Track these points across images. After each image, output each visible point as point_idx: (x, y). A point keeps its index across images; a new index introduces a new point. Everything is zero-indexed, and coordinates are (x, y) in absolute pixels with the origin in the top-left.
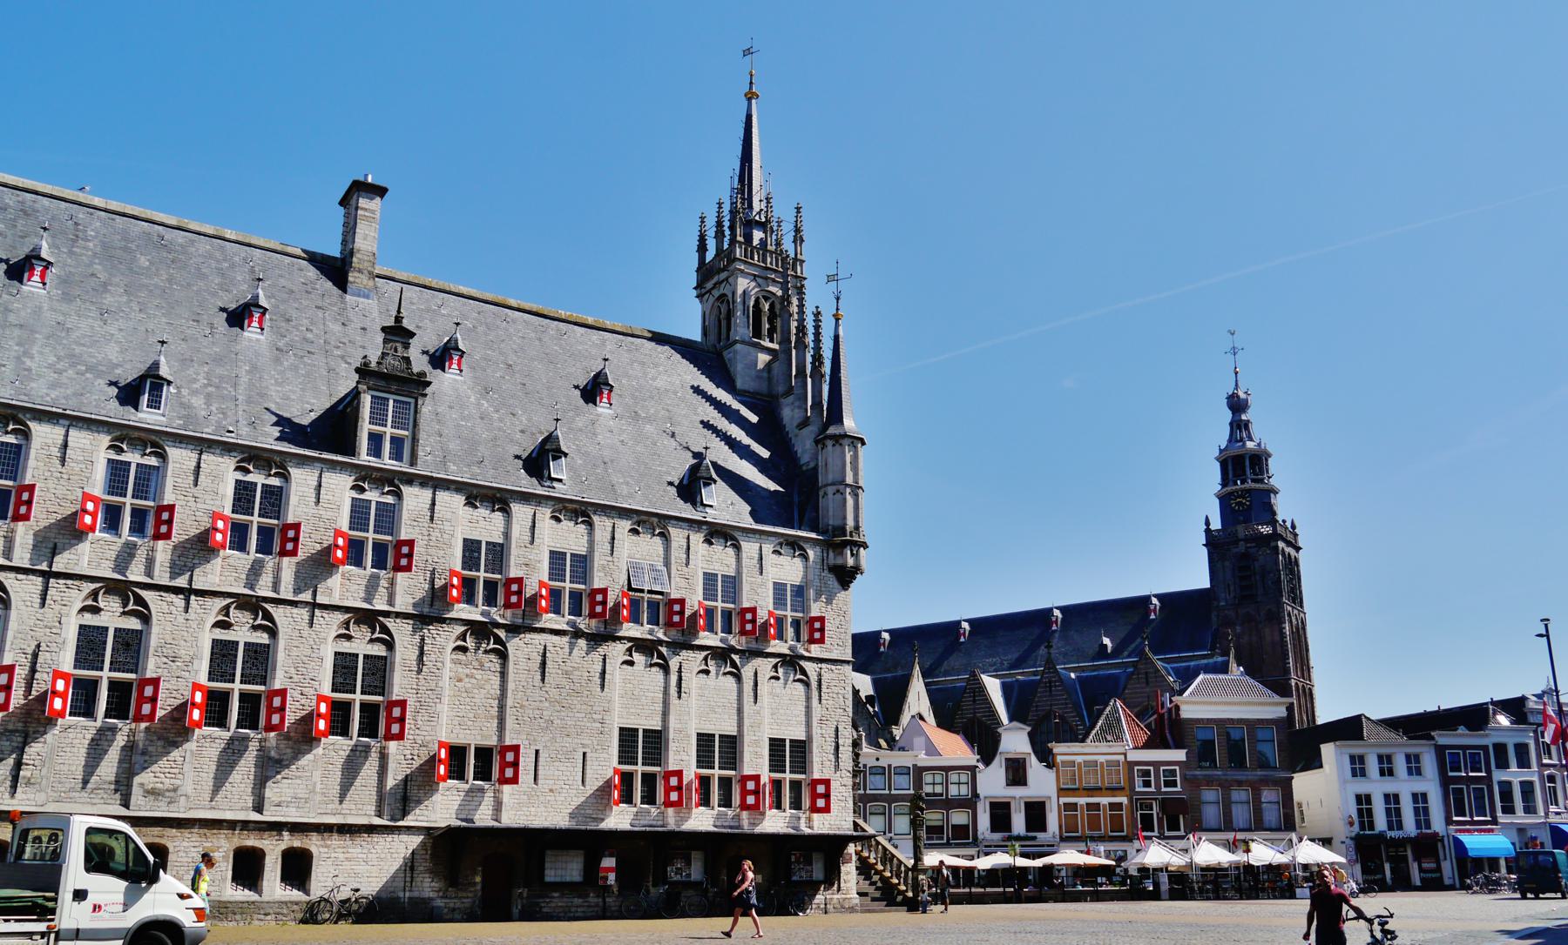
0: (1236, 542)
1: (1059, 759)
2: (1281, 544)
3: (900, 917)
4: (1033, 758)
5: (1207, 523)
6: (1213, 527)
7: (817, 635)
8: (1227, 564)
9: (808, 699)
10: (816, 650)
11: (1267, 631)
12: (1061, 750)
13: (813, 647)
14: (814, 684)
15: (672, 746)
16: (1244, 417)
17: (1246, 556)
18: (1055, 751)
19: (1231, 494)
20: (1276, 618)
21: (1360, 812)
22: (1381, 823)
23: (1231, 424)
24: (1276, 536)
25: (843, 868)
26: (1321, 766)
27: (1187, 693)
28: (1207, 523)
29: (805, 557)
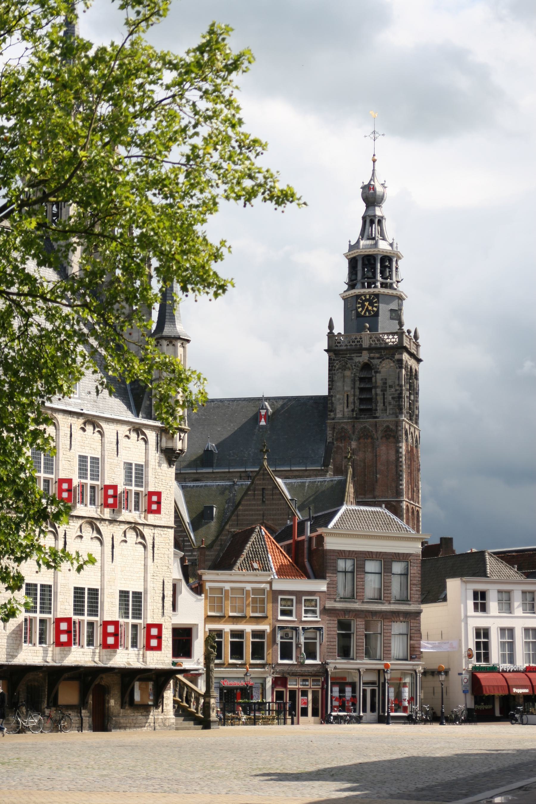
0: (360, 350)
1: (208, 585)
2: (405, 356)
3: (197, 735)
4: (184, 582)
5: (331, 326)
6: (335, 332)
7: (154, 507)
8: (348, 373)
9: (145, 558)
10: (152, 519)
11: (382, 450)
12: (212, 578)
13: (151, 516)
14: (150, 547)
15: (59, 597)
16: (378, 212)
17: (367, 367)
18: (204, 578)
19: (358, 296)
20: (393, 434)
21: (478, 644)
22: (495, 658)
23: (364, 218)
24: (400, 348)
25: (165, 695)
26: (445, 599)
27: (331, 525)
28: (331, 326)
29: (146, 441)
